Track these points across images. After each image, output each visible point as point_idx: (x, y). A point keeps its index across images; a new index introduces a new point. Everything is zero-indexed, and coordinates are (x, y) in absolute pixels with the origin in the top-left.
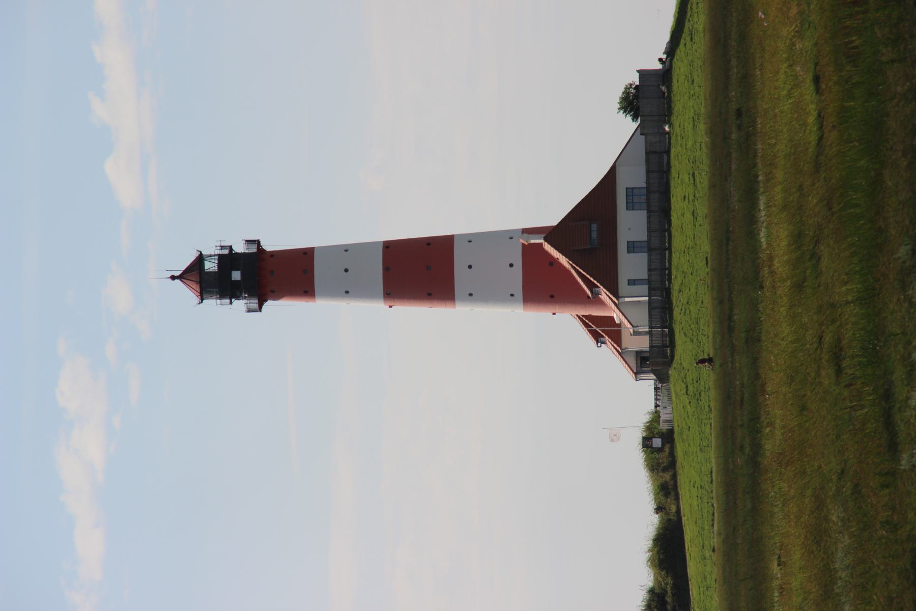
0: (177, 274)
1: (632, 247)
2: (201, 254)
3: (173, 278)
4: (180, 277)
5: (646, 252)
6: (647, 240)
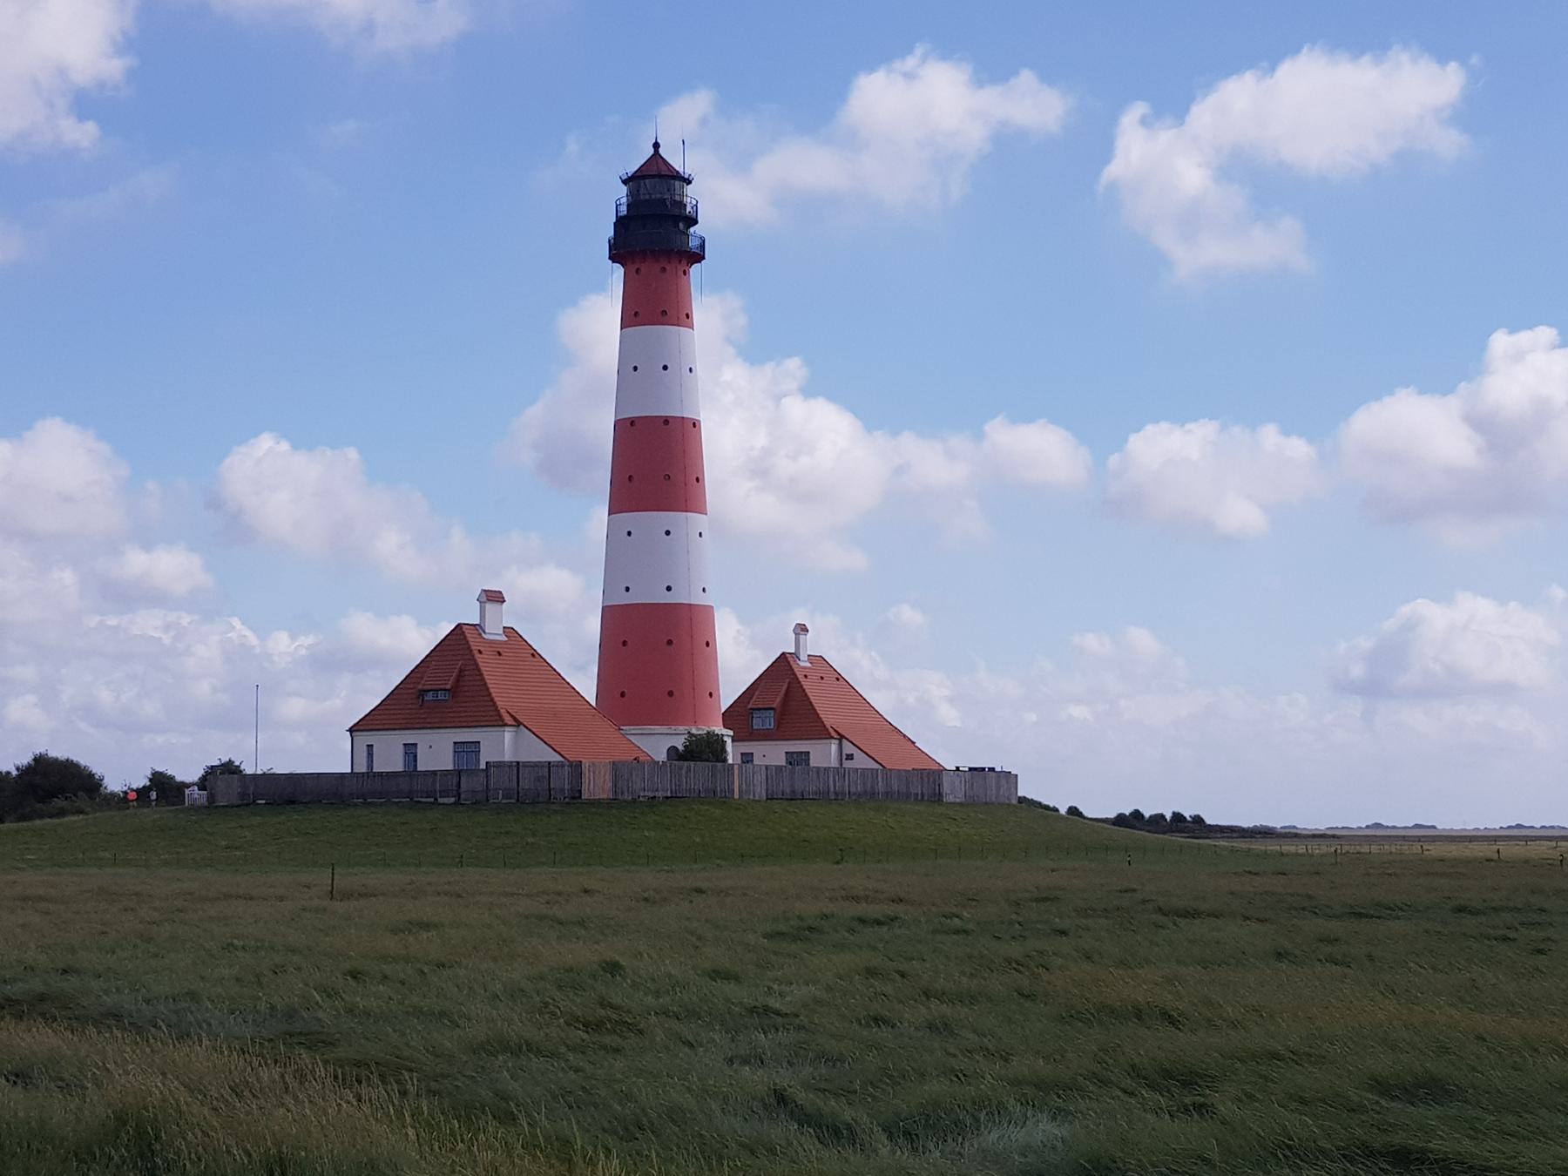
0: (661, 151)
1: (410, 751)
2: (689, 182)
3: (656, 146)
5: (352, 769)
6: (419, 769)
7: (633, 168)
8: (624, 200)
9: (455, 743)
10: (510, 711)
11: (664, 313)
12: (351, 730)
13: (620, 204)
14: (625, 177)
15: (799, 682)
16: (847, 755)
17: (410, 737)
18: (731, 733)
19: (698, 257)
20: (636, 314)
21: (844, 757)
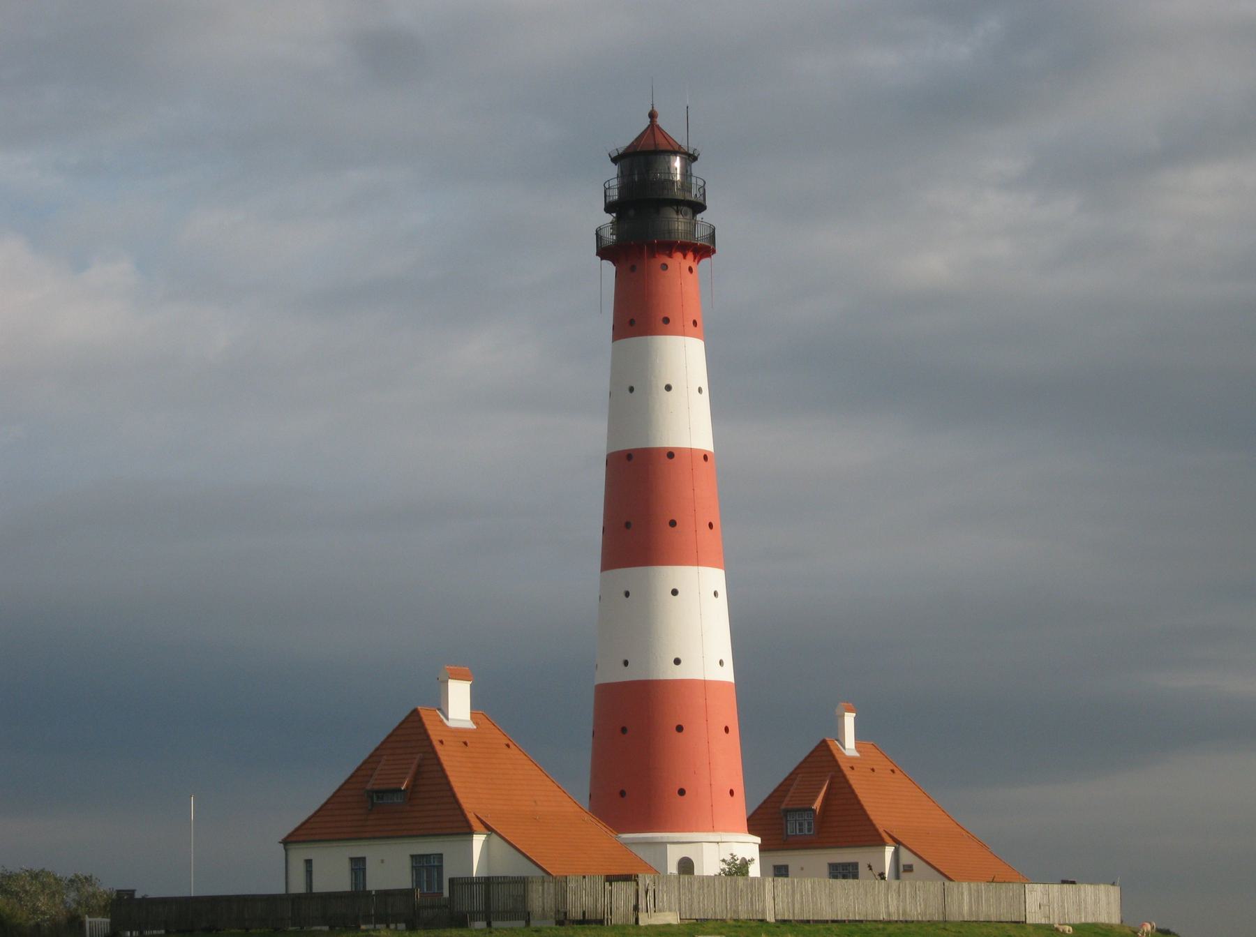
0: (660, 121)
1: (358, 866)
3: (652, 115)
4: (653, 127)
7: (624, 140)
8: (614, 183)
9: (412, 856)
10: (479, 815)
11: (666, 320)
12: (287, 842)
13: (609, 188)
14: (614, 154)
15: (844, 776)
16: (904, 866)
17: (358, 850)
18: (758, 840)
19: (704, 251)
20: (632, 322)
21: (901, 869)
